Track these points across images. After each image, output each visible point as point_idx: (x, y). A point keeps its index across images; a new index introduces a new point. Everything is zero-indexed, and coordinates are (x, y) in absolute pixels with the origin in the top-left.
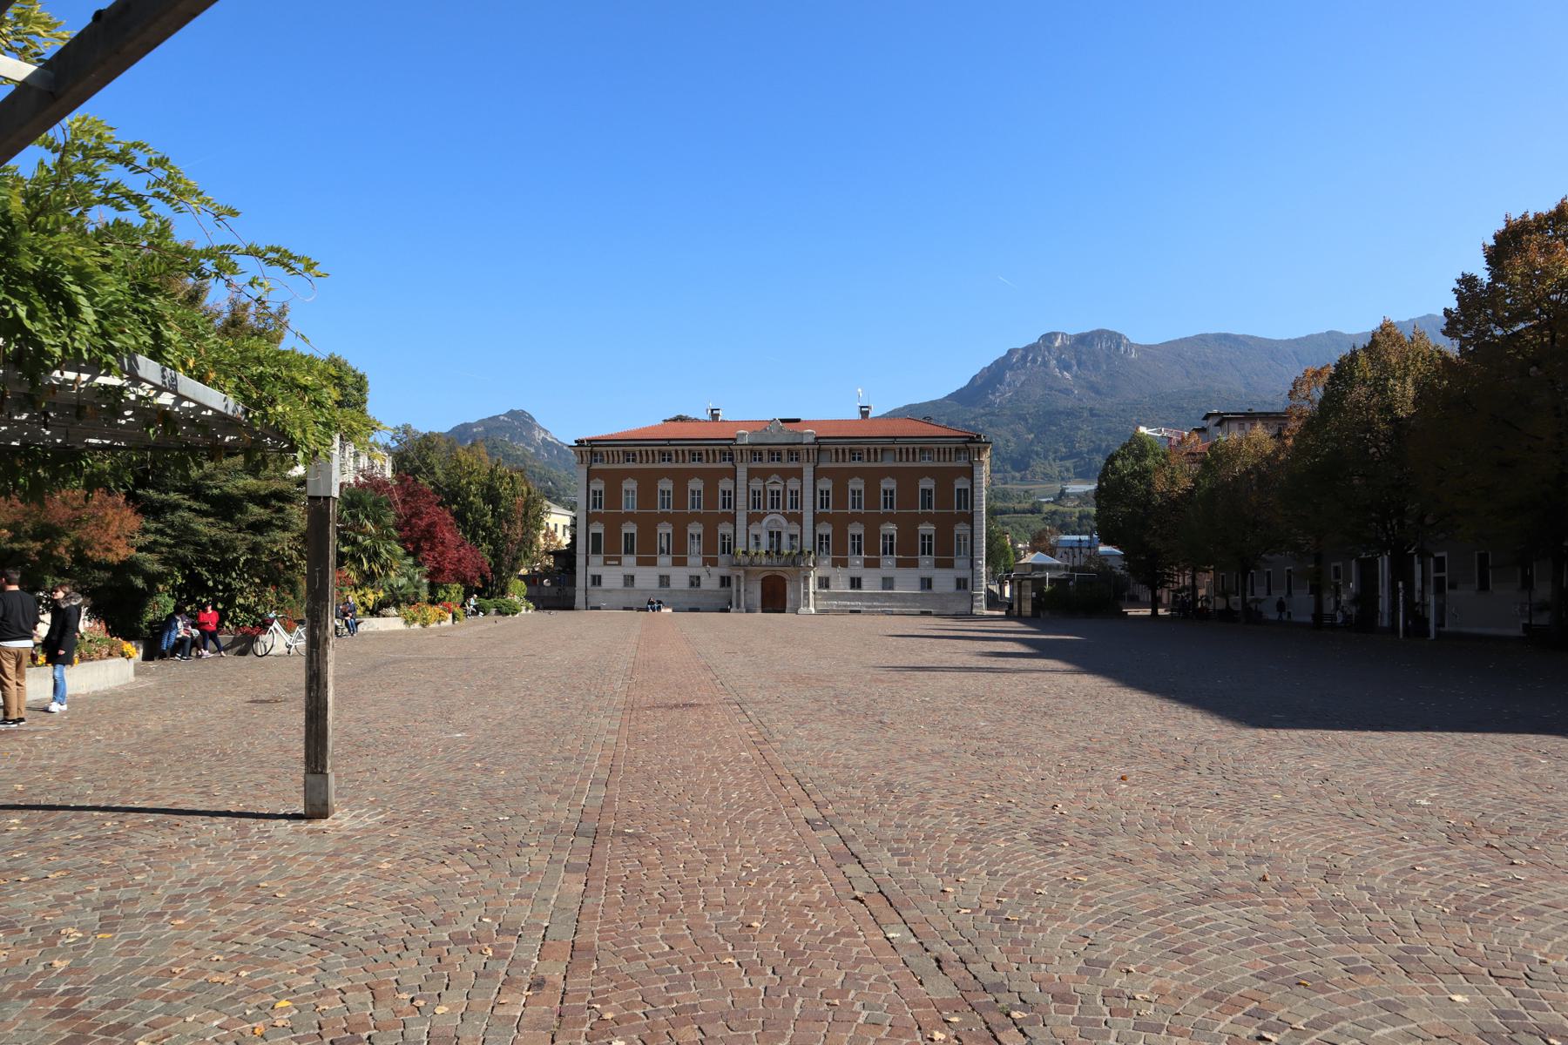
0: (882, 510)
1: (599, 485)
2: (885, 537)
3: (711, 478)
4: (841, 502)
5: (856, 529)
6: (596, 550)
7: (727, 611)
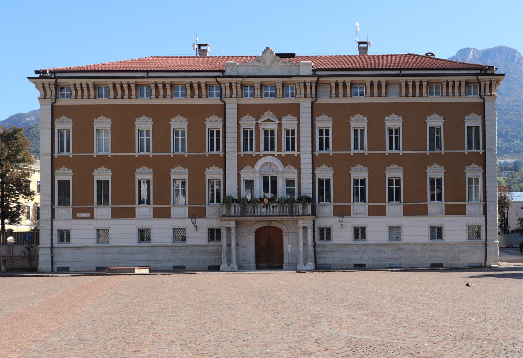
0: (387, 152)
1: (65, 125)
2: (391, 181)
3: (196, 115)
4: (342, 142)
5: (359, 172)
6: (64, 201)
7: (216, 268)
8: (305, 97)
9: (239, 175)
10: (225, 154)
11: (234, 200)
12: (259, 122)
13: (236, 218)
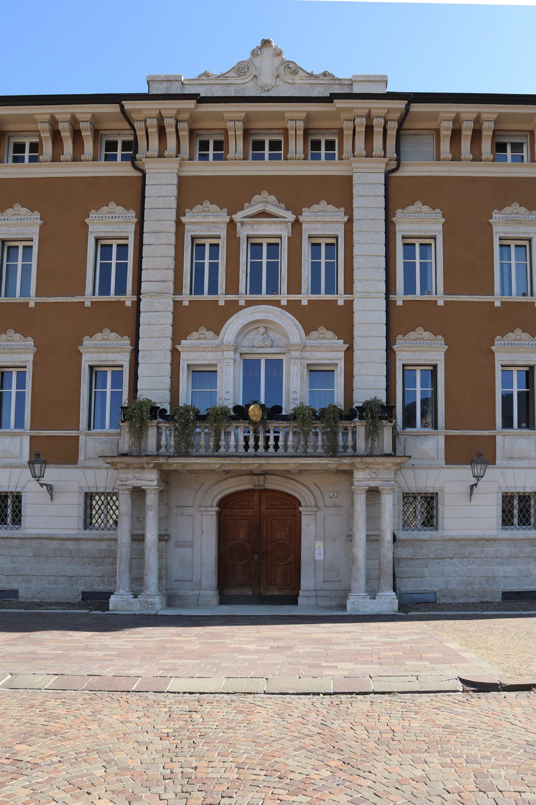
8: (369, 154)
9: (175, 353)
10: (139, 300)
11: (155, 412)
12: (238, 217)
13: (162, 460)
